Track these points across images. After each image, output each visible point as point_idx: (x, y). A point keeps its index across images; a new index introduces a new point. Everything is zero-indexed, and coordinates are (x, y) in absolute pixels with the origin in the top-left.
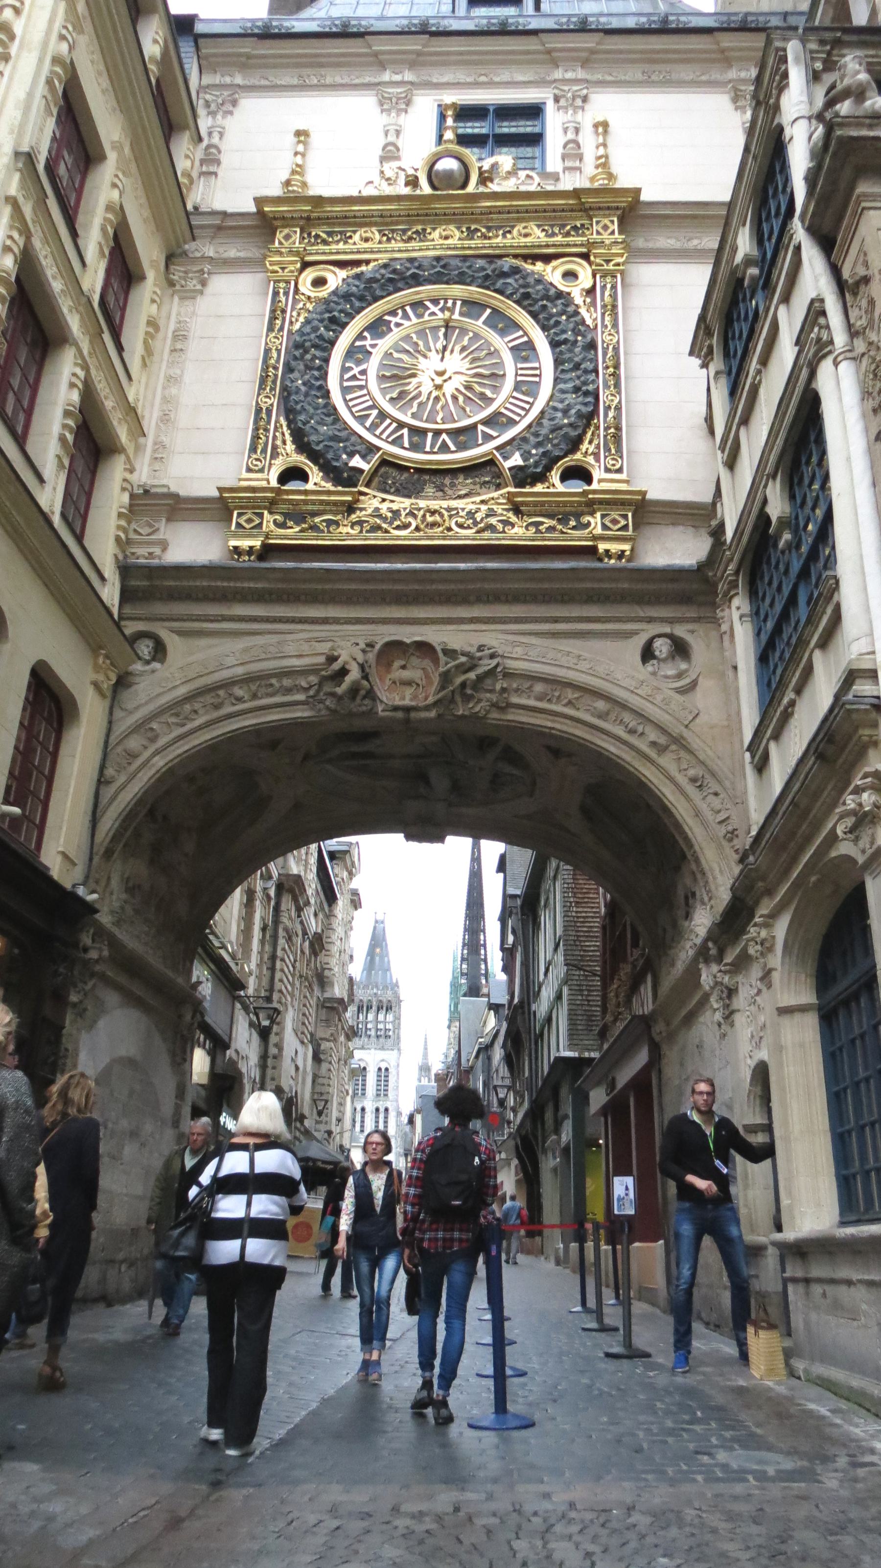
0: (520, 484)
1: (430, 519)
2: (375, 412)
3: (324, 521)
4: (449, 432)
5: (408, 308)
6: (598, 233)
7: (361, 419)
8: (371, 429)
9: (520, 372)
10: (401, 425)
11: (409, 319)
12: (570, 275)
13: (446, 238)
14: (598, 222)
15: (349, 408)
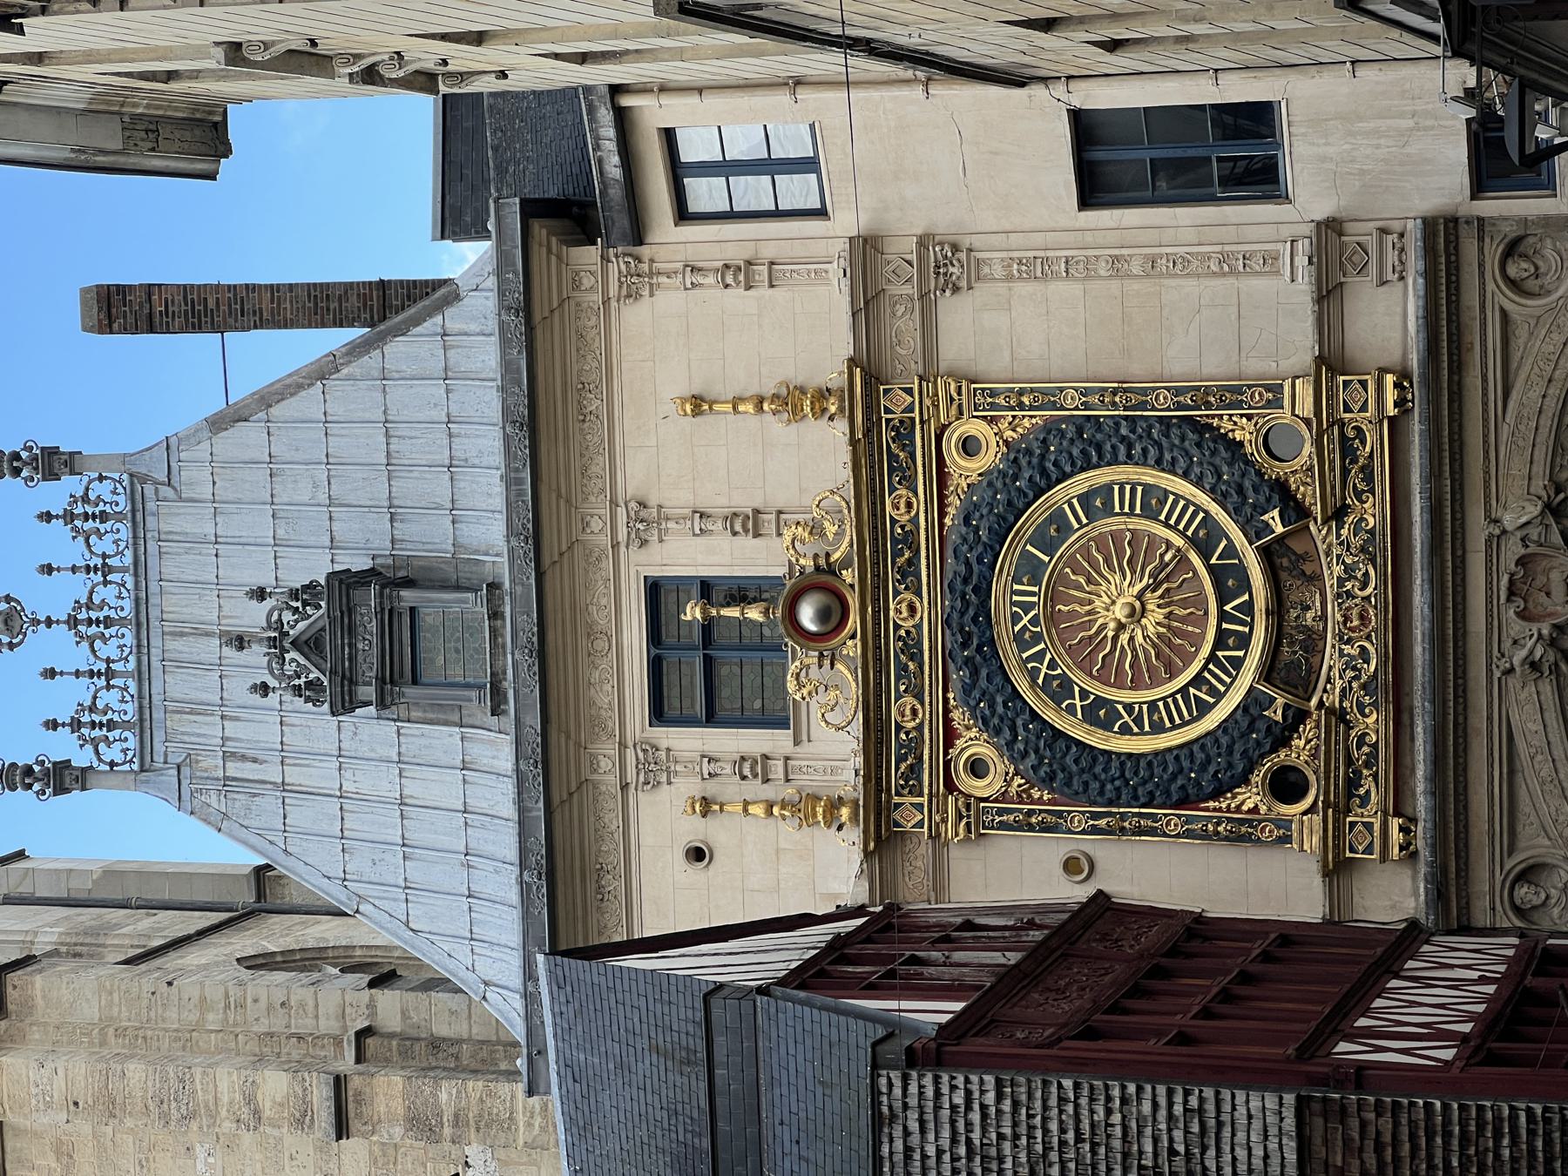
0: (1303, 513)
1: (1356, 623)
2: (1192, 690)
3: (1359, 748)
4: (1222, 601)
5: (1025, 656)
6: (910, 409)
7: (1204, 708)
8: (1219, 696)
9: (1126, 510)
10: (1212, 658)
11: (1042, 653)
12: (969, 447)
13: (912, 609)
14: (888, 411)
15: (1185, 724)
